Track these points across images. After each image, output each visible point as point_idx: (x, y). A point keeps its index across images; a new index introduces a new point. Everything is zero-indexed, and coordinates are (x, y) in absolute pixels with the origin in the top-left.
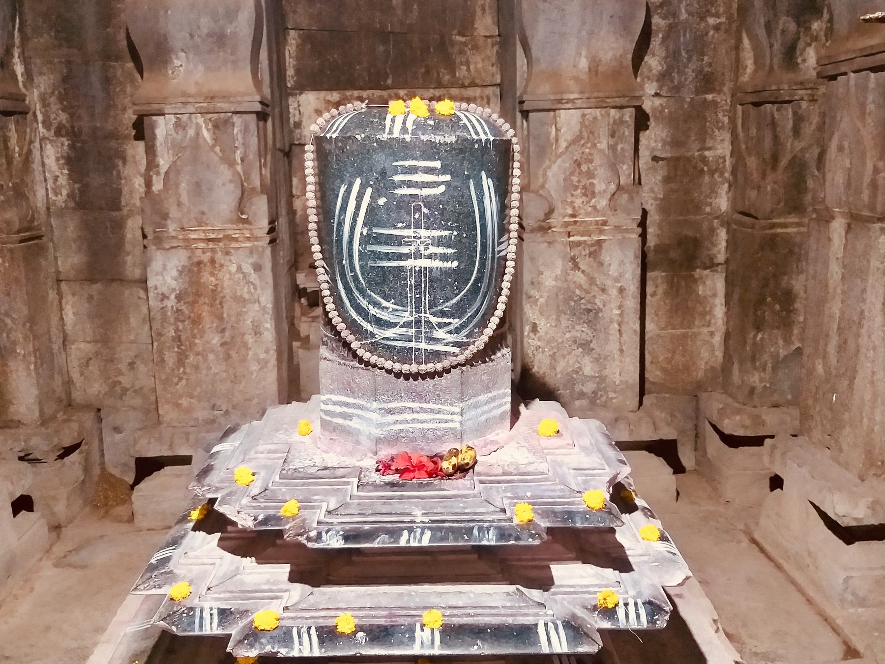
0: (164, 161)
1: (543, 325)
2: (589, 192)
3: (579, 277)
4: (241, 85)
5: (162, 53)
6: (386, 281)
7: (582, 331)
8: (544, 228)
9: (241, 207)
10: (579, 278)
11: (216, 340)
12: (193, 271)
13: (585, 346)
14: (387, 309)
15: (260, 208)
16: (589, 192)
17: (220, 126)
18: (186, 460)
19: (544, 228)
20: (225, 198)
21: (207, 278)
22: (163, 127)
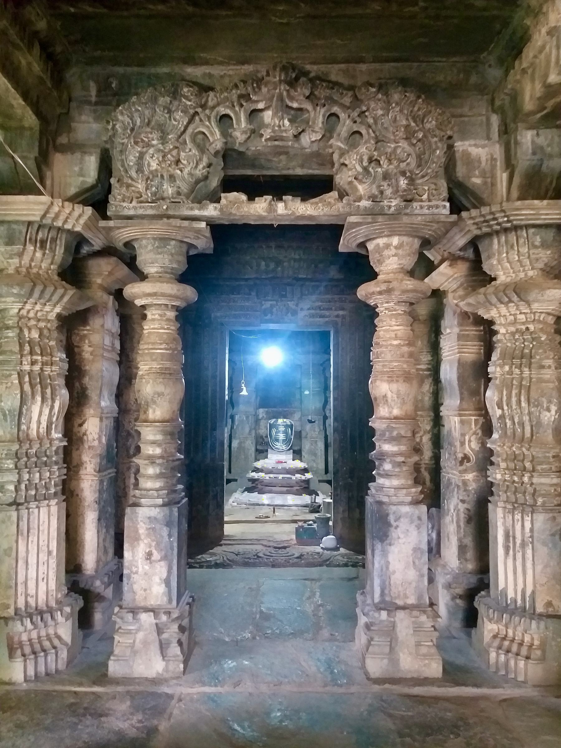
0: (236, 423)
1: (306, 456)
2: (315, 431)
3: (313, 447)
4: (251, 410)
5: (238, 404)
6: (277, 440)
7: (314, 458)
8: (306, 437)
9: (250, 431)
10: (313, 447)
11: (243, 457)
12: (240, 444)
13: (314, 461)
14: (277, 444)
15: (253, 432)
16: (315, 431)
17: (247, 417)
18: (236, 480)
19: (306, 437)
20: (247, 430)
21: (243, 445)
22: (237, 417)
